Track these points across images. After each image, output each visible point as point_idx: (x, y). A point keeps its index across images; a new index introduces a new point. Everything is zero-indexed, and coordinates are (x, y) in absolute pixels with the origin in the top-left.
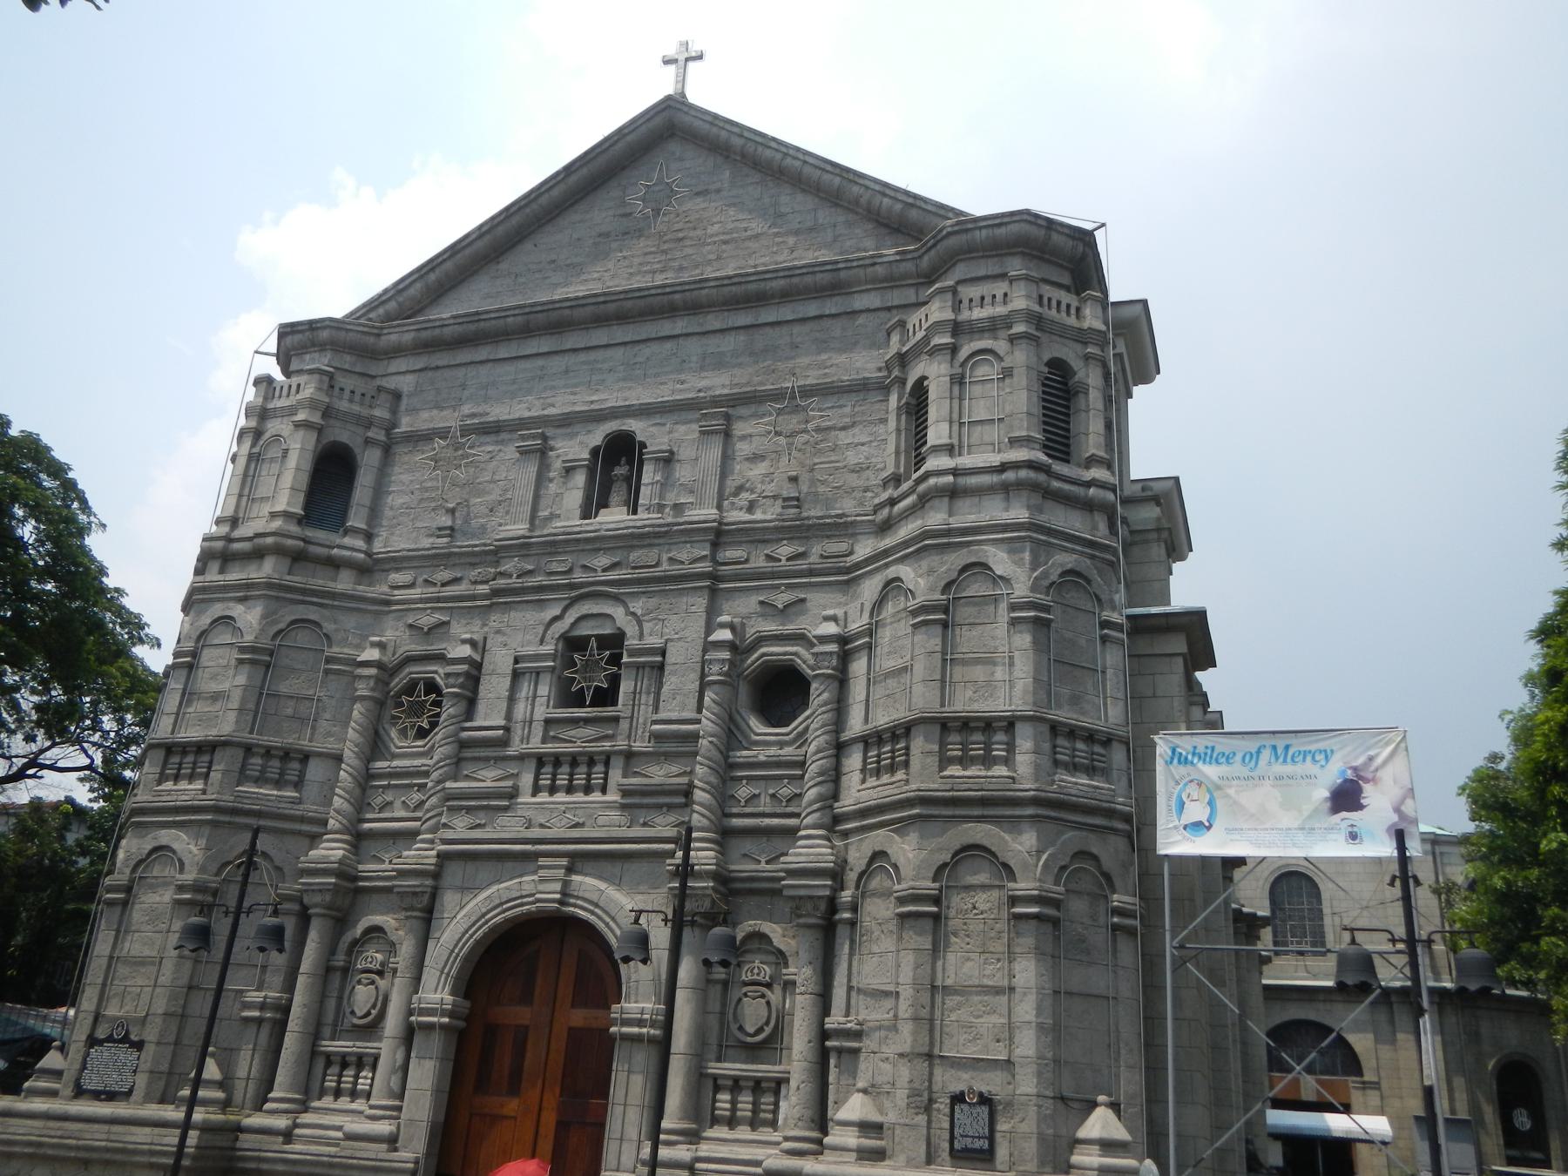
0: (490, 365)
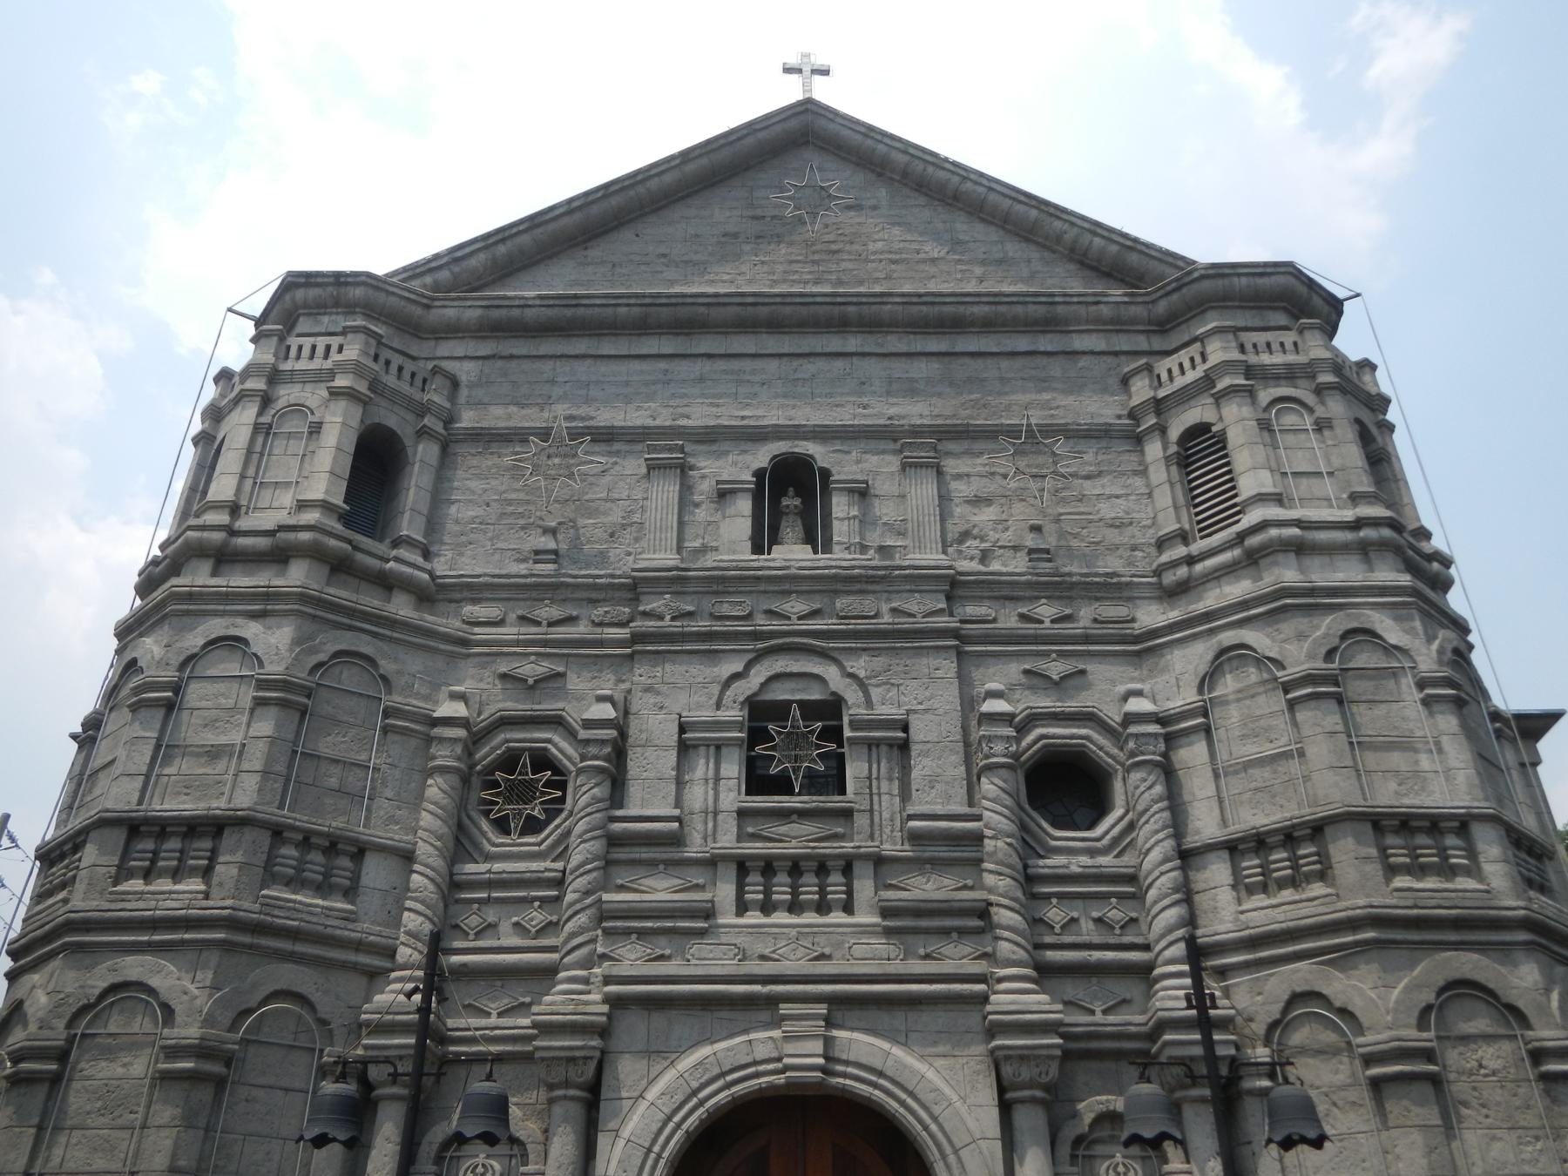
0: (589, 362)
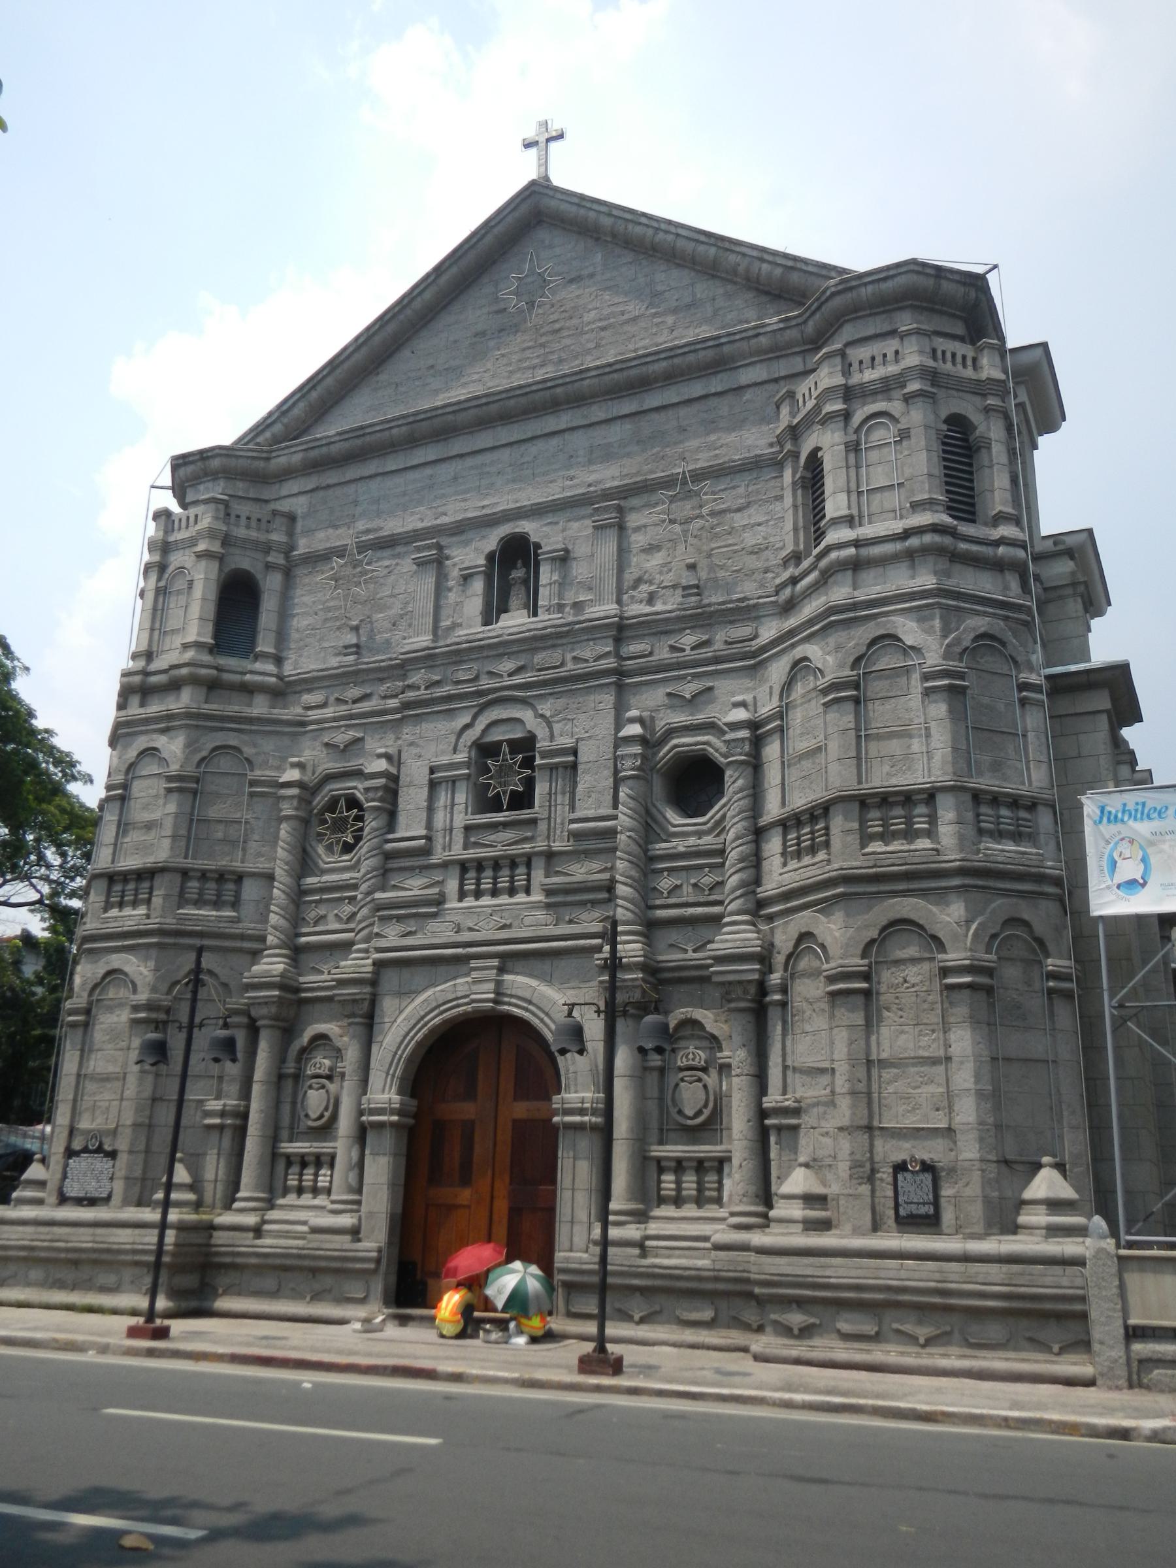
0: (379, 479)
